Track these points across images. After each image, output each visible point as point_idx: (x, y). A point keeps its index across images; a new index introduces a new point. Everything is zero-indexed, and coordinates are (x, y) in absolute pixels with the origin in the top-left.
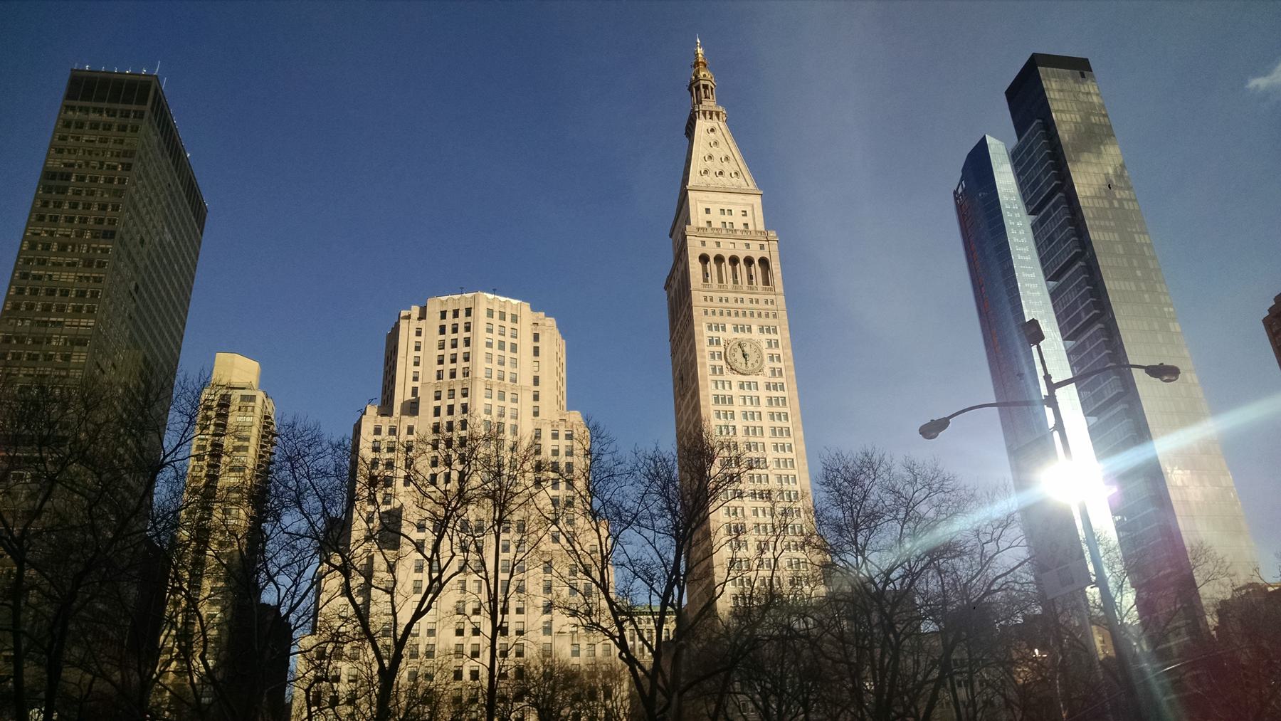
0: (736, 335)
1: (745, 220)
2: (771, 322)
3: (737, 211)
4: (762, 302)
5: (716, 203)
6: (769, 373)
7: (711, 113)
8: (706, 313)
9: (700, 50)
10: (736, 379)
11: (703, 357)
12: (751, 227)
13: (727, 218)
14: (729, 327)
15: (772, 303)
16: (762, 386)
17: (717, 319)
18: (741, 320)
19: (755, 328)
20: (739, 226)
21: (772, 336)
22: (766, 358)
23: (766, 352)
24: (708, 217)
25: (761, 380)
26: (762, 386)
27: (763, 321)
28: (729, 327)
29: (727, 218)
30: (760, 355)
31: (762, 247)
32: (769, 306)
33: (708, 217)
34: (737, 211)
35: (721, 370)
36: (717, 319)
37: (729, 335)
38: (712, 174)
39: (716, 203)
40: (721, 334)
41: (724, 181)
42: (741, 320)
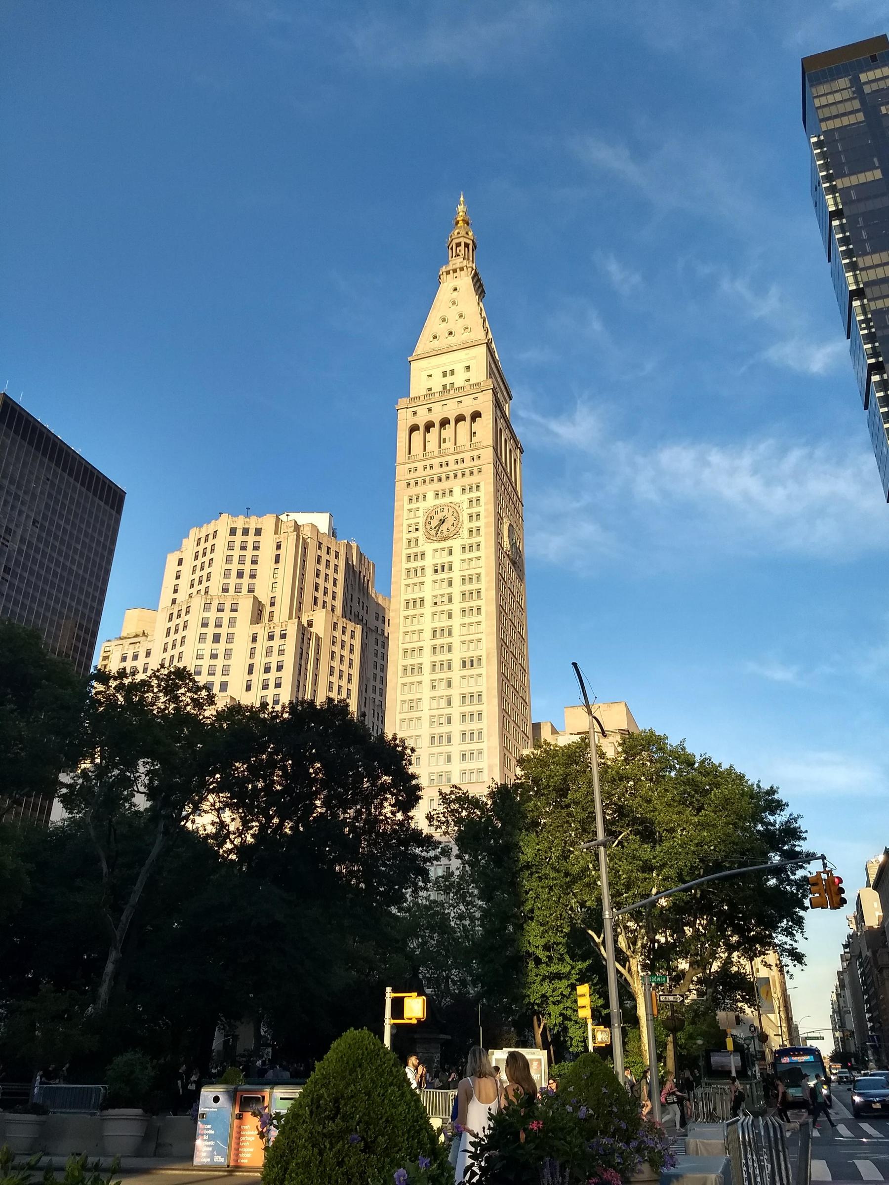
0: (438, 502)
1: (467, 375)
3: (459, 368)
5: (438, 366)
6: (465, 533)
13: (449, 380)
14: (430, 495)
19: (457, 490)
26: (457, 550)
27: (468, 480)
28: (430, 495)
29: (449, 380)
34: (459, 368)
37: (431, 501)
39: (438, 366)
40: (422, 505)
42: (445, 485)
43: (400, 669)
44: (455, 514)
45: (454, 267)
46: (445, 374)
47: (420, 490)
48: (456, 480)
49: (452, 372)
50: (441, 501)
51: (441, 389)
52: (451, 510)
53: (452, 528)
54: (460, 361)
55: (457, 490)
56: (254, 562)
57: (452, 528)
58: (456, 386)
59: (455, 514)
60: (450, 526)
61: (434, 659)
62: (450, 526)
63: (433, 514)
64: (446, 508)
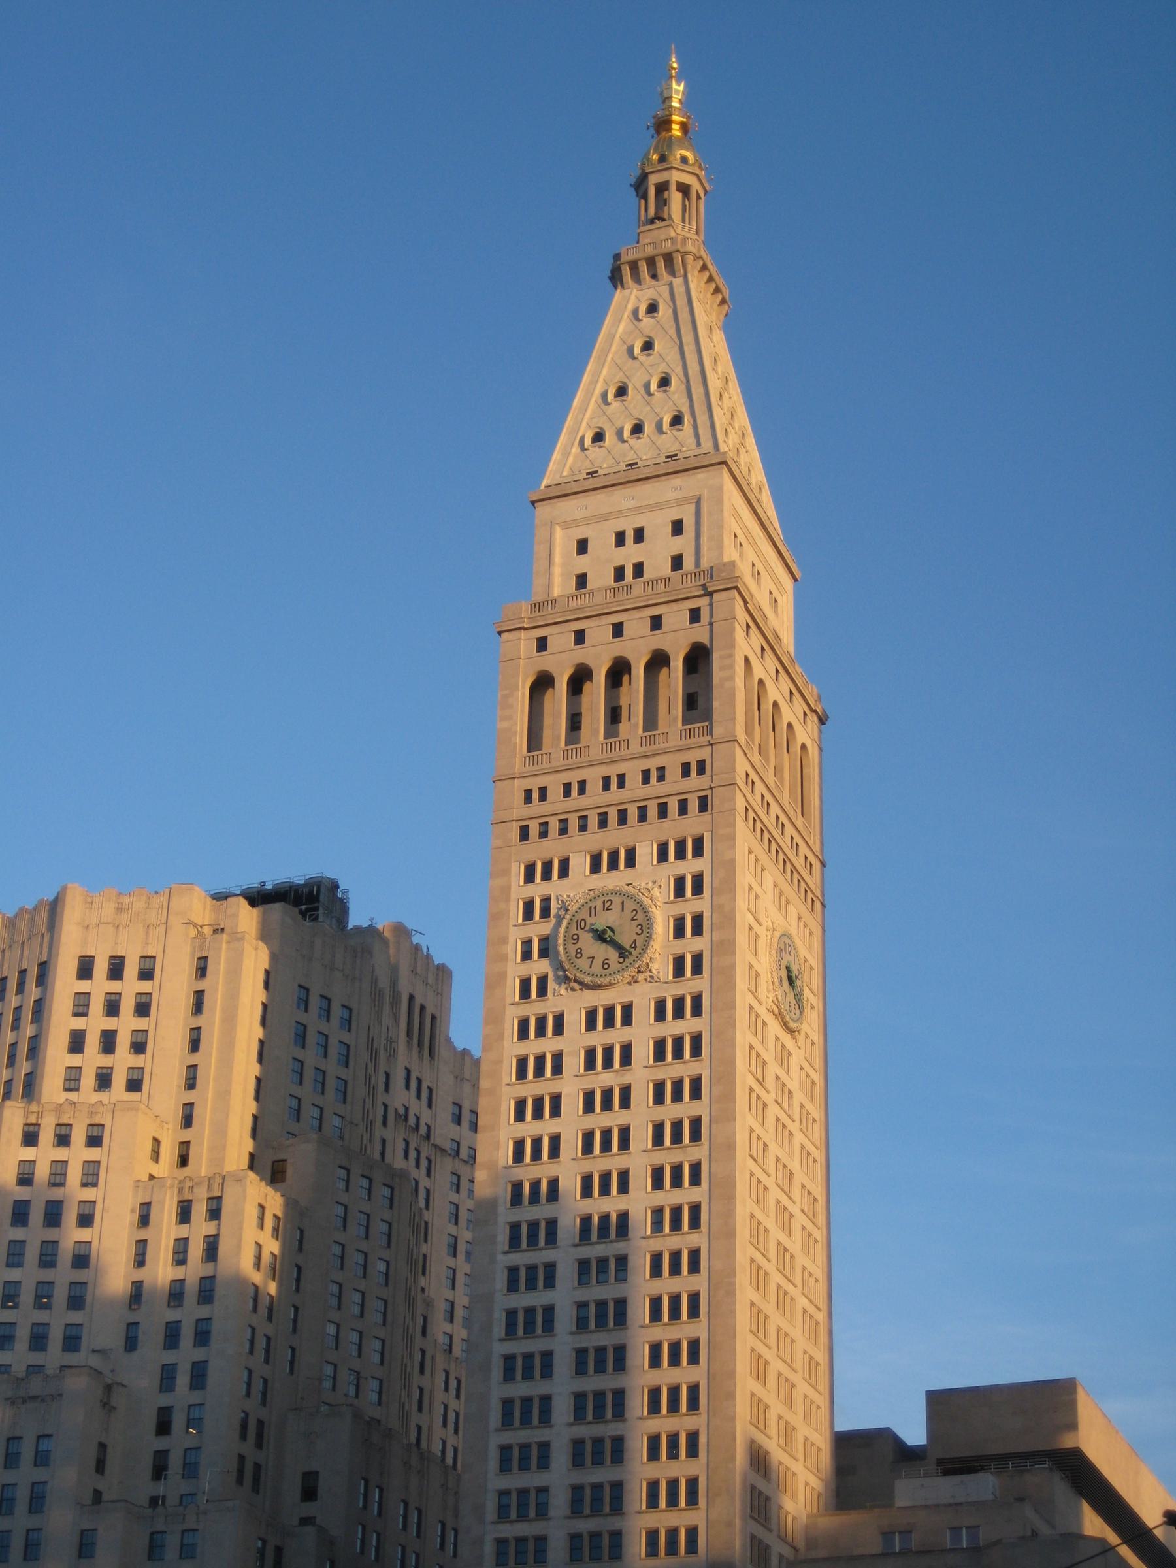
4: (633, 780)
5: (603, 518)
6: (662, 967)
7: (651, 262)
8: (524, 833)
9: (678, 89)
11: (503, 958)
12: (688, 564)
13: (630, 554)
14: (580, 864)
15: (701, 767)
16: (644, 1013)
17: (553, 848)
18: (615, 838)
19: (646, 853)
20: (658, 565)
21: (689, 866)
22: (662, 927)
24: (582, 564)
25: (643, 999)
26: (644, 1013)
27: (675, 828)
28: (580, 864)
29: (630, 554)
30: (645, 928)
31: (695, 616)
33: (582, 564)
34: (658, 525)
35: (543, 981)
38: (610, 438)
39: (603, 518)
40: (556, 888)
41: (644, 450)
43: (500, 1318)
44: (640, 916)
45: (649, 251)
46: (620, 539)
47: (553, 848)
48: (645, 826)
49: (639, 535)
50: (608, 880)
51: (610, 580)
52: (630, 905)
54: (657, 507)
55: (646, 853)
56: (143, 1009)
58: (648, 574)
59: (640, 916)
61: (584, 1295)
63: (584, 914)
64: (617, 900)
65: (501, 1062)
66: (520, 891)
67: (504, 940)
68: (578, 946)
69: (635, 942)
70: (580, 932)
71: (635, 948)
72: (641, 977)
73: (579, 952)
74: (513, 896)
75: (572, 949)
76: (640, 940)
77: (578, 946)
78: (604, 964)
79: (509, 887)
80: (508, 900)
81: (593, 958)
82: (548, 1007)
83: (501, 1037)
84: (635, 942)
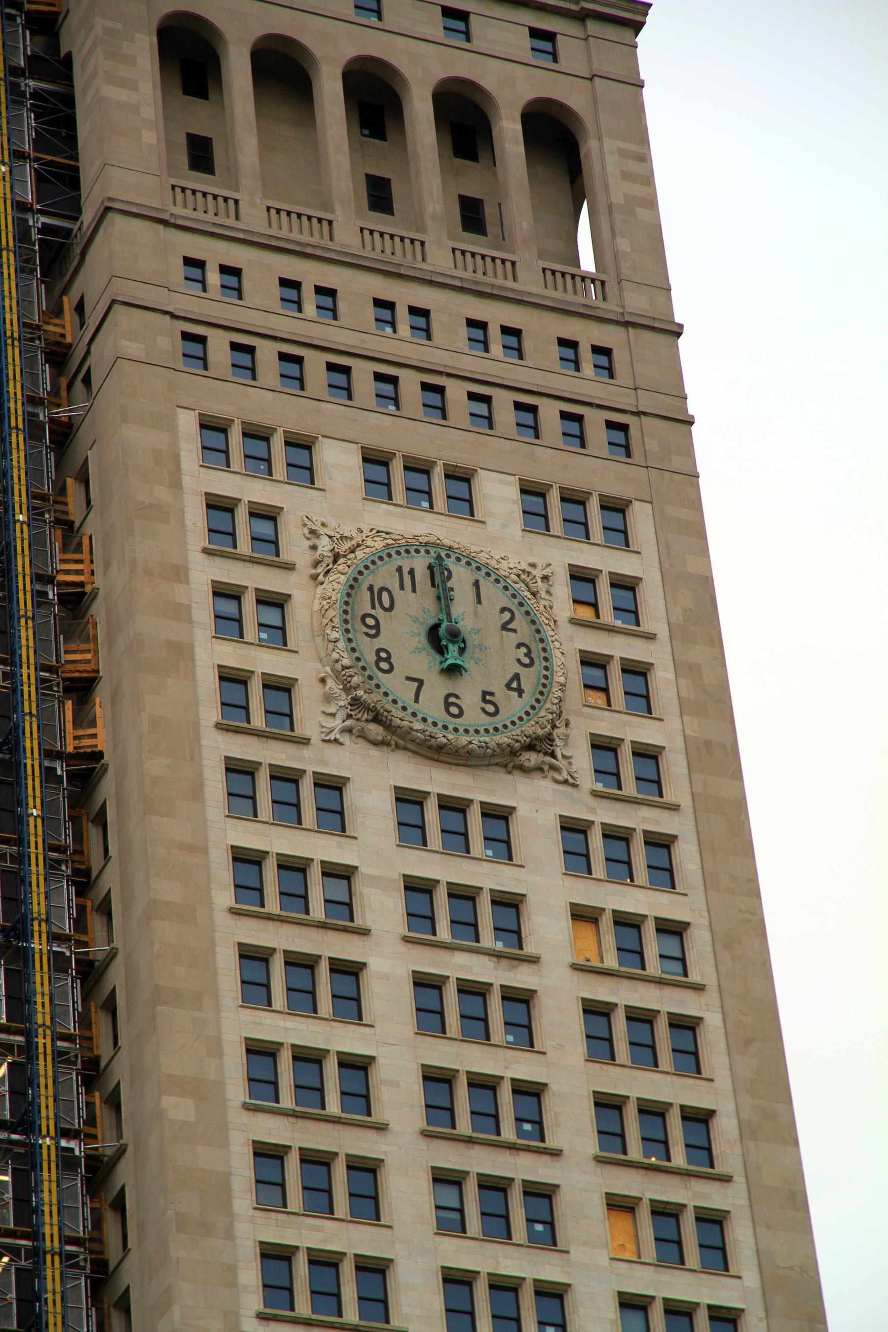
2: (597, 472)
10: (374, 780)
14: (338, 462)
19: (498, 494)
23: (569, 643)
28: (338, 462)
32: (587, 383)
36: (265, 402)
53: (512, 706)
55: (498, 494)
57: (512, 706)
60: (498, 687)
62: (498, 687)
63: (384, 576)
65: (205, 851)
66: (200, 480)
67: (180, 574)
68: (379, 643)
69: (517, 677)
70: (379, 612)
71: (520, 691)
72: (532, 758)
73: (384, 658)
74: (187, 481)
75: (368, 648)
76: (529, 679)
77: (379, 643)
78: (447, 705)
79: (177, 458)
80: (176, 485)
81: (421, 682)
82: (311, 761)
83: (197, 793)
84: (517, 677)
